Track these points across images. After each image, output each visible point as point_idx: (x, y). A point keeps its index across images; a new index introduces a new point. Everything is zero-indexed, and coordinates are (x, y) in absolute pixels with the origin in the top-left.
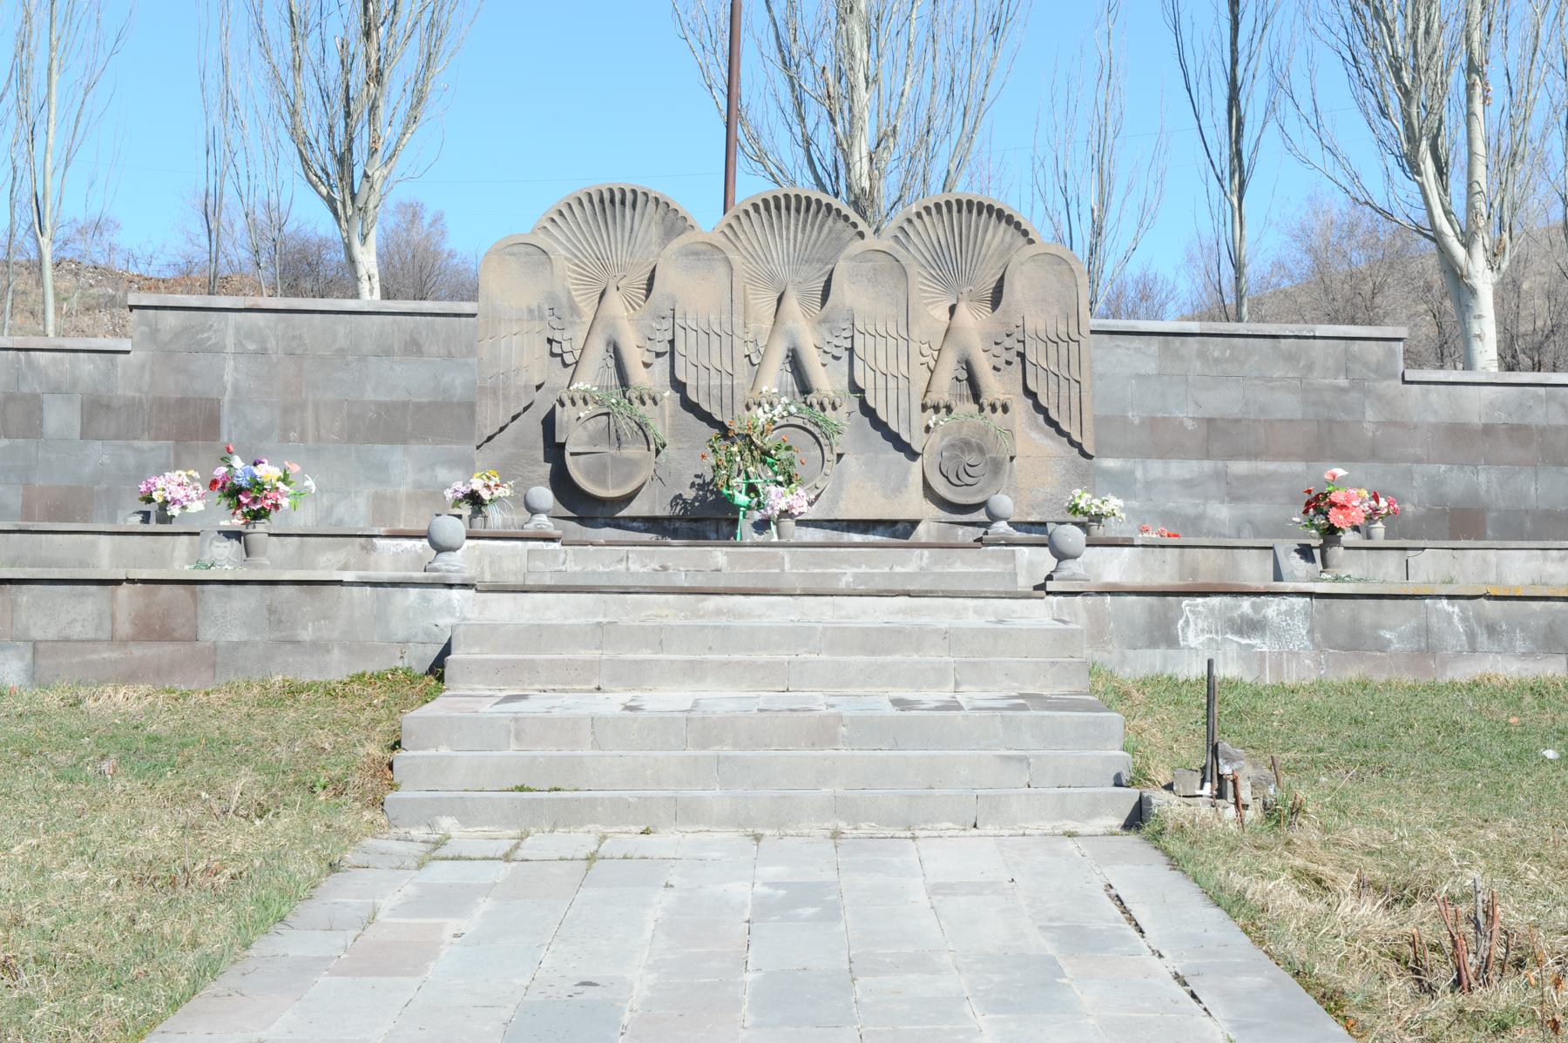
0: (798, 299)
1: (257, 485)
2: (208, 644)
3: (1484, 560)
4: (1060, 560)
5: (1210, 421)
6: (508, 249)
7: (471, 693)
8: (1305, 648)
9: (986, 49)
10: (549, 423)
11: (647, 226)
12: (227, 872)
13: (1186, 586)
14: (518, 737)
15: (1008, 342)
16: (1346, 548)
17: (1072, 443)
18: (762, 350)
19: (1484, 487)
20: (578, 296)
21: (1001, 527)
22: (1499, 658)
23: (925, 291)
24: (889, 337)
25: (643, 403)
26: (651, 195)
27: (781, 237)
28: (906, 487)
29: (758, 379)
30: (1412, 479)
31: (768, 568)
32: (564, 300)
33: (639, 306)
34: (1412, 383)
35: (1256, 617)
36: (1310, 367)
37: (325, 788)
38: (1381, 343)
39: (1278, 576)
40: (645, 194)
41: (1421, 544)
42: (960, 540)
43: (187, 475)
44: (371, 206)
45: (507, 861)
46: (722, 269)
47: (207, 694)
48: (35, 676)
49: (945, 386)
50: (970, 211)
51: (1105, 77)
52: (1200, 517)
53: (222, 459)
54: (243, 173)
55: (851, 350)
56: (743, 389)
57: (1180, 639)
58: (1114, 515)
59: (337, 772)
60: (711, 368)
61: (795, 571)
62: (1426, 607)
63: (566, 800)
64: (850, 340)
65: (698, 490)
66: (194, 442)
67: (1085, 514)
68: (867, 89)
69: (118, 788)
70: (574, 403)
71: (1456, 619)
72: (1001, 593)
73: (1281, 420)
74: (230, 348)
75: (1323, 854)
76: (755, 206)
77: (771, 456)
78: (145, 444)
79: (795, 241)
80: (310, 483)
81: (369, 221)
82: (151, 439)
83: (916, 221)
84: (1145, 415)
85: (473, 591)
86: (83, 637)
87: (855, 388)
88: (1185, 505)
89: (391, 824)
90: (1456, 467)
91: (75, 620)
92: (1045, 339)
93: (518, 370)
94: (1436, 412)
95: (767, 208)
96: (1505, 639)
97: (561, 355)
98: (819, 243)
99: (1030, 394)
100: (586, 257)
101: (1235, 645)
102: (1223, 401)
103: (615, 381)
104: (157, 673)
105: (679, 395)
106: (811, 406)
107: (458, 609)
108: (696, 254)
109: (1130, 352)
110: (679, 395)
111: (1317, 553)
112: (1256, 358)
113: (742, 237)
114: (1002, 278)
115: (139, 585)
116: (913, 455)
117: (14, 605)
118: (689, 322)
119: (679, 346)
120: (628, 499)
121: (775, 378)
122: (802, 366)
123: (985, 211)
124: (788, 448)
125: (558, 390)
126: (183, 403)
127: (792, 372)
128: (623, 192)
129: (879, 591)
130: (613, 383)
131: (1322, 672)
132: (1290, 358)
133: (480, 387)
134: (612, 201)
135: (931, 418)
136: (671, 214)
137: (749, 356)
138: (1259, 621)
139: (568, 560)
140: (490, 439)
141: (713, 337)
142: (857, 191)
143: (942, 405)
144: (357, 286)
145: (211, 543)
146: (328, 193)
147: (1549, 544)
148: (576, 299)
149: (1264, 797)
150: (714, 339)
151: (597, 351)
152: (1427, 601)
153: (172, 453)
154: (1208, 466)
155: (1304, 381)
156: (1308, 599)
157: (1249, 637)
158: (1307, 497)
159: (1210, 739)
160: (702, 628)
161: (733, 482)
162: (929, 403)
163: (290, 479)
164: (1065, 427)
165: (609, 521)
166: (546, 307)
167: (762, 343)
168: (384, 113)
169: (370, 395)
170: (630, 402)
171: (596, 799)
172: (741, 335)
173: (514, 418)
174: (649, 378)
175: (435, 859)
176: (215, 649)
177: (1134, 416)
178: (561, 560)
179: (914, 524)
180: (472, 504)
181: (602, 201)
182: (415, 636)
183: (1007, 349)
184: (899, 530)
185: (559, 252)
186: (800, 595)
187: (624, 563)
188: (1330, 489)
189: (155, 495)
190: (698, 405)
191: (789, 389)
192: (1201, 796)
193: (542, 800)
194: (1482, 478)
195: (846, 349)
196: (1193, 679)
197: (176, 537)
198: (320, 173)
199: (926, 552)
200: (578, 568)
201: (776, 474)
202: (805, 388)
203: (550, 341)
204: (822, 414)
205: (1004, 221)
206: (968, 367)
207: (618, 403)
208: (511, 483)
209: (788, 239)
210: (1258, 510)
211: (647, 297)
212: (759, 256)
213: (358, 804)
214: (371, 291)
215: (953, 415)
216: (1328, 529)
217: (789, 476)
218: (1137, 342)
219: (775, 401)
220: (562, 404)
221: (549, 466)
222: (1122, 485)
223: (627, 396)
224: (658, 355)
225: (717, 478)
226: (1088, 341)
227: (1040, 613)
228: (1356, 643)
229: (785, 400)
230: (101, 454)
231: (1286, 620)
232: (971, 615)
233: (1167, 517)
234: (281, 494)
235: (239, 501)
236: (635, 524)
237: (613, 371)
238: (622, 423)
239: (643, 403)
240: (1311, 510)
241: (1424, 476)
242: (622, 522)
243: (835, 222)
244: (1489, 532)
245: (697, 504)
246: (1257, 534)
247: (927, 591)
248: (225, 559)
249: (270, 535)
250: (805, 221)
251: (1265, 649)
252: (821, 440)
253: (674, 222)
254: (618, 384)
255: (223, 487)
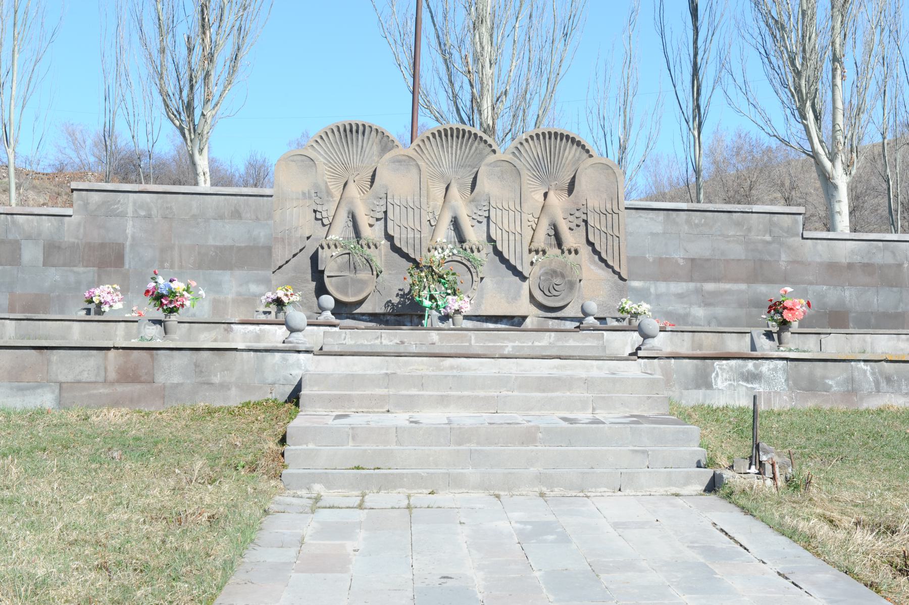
0: (458, 188)
1: (172, 293)
2: (160, 385)
3: (864, 340)
4: (644, 339)
5: (693, 260)
6: (291, 158)
7: (315, 413)
8: (784, 390)
9: (559, 45)
10: (314, 259)
11: (371, 145)
12: (206, 515)
13: (717, 353)
14: (354, 438)
15: (578, 214)
16: (792, 333)
17: (614, 272)
18: (437, 217)
19: (848, 299)
20: (331, 185)
21: (590, 320)
22: (893, 396)
23: (530, 184)
24: (510, 211)
25: (369, 247)
26: (374, 127)
27: (448, 152)
28: (520, 297)
29: (435, 234)
30: (807, 294)
31: (462, 343)
32: (323, 187)
33: (367, 191)
34: (807, 239)
35: (756, 372)
36: (749, 230)
37: (243, 467)
38: (790, 216)
39: (753, 348)
40: (370, 127)
41: (829, 331)
42: (550, 327)
43: (113, 288)
44: (205, 132)
45: (361, 509)
46: (414, 171)
47: (161, 413)
48: (60, 402)
49: (541, 239)
50: (556, 138)
51: (628, 62)
52: (687, 315)
53: (152, 278)
54: (131, 113)
55: (488, 218)
56: (426, 240)
57: (713, 384)
58: (645, 313)
59: (250, 458)
60: (408, 227)
61: (478, 344)
62: (852, 366)
63: (386, 474)
64: (487, 212)
65: (401, 298)
66: (108, 269)
67: (628, 313)
68: (490, 67)
69: (128, 466)
70: (329, 247)
71: (868, 374)
72: (612, 357)
73: (733, 260)
74: (130, 214)
75: (830, 506)
76: (433, 134)
77: (444, 279)
78: (81, 269)
79: (456, 155)
80: (202, 292)
81: (204, 140)
82: (83, 266)
83: (525, 144)
84: (656, 256)
85: (312, 354)
86: (89, 380)
87: (490, 240)
88: (678, 308)
89: (287, 488)
90: (832, 287)
91: (84, 370)
92: (599, 212)
93: (296, 228)
94: (821, 256)
95: (440, 136)
96: (896, 385)
97: (321, 220)
98: (470, 156)
99: (590, 243)
101: (744, 388)
102: (700, 249)
103: (352, 235)
104: (131, 401)
105: (389, 243)
106: (465, 250)
107: (303, 365)
108: (399, 161)
109: (648, 220)
110: (389, 243)
111: (775, 336)
112: (719, 224)
113: (425, 152)
114: (574, 177)
115: (121, 350)
116: (524, 278)
117: (49, 362)
118: (395, 201)
119: (390, 215)
120: (360, 303)
121: (444, 233)
122: (460, 227)
123: (565, 138)
124: (454, 274)
125: (320, 240)
126: (103, 245)
127: (454, 230)
128: (357, 125)
129: (542, 356)
130: (352, 236)
131: (793, 403)
132: (738, 224)
133: (275, 238)
134: (351, 131)
135: (535, 258)
136: (385, 139)
137: (429, 221)
138: (758, 374)
139: (347, 337)
140: (280, 267)
141: (409, 209)
142: (485, 126)
143: (540, 250)
144: (197, 178)
145: (145, 327)
146: (180, 124)
147: (900, 331)
148: (331, 187)
149: (786, 474)
150: (410, 211)
151: (343, 217)
152: (852, 363)
153: (96, 275)
154: (692, 285)
155: (747, 237)
156: (785, 362)
157: (752, 383)
158: (770, 304)
159: (755, 441)
160: (446, 376)
161: (422, 293)
162: (533, 249)
163: (191, 290)
164: (610, 263)
165: (348, 315)
166: (313, 191)
167: (437, 213)
168: (213, 79)
169: (211, 242)
170: (362, 246)
171: (403, 474)
172: (425, 209)
173: (294, 256)
174: (372, 233)
175: (319, 508)
176: (164, 387)
177: (650, 257)
178: (343, 338)
179: (524, 318)
180: (277, 305)
181: (345, 130)
182: (278, 381)
183: (577, 218)
184: (515, 321)
185: (320, 160)
186: (498, 358)
187: (379, 339)
188: (783, 299)
189: (94, 299)
190: (400, 249)
191: (453, 240)
192: (749, 473)
193: (372, 474)
194: (847, 293)
195: (485, 217)
196: (721, 407)
197: (117, 323)
198: (175, 113)
199: (553, 334)
200: (353, 342)
201: (447, 289)
202: (462, 240)
203: (315, 211)
204: (472, 254)
205: (575, 144)
206: (555, 227)
207: (355, 247)
208: (300, 293)
209: (452, 154)
210: (720, 311)
211: (371, 186)
212: (435, 163)
213: (265, 477)
214: (205, 181)
215: (547, 255)
216: (782, 322)
217: (454, 290)
218: (651, 213)
219: (445, 247)
220: (323, 248)
221: (314, 283)
222: (641, 295)
223: (360, 243)
224: (378, 220)
225: (413, 291)
226: (624, 213)
227: (634, 368)
228: (813, 387)
229: (450, 246)
230: (54, 275)
231: (773, 374)
232: (596, 370)
233: (668, 315)
234: (185, 298)
235: (161, 302)
236: (364, 317)
237: (351, 229)
238: (357, 258)
239: (369, 247)
240: (772, 311)
241: (814, 293)
242: (356, 316)
243: (479, 144)
244: (851, 325)
245: (400, 306)
246: (720, 324)
247: (570, 356)
248: (153, 335)
249: (179, 322)
250: (462, 143)
251: (761, 390)
252: (472, 269)
253: (386, 143)
254: (354, 236)
255: (152, 294)
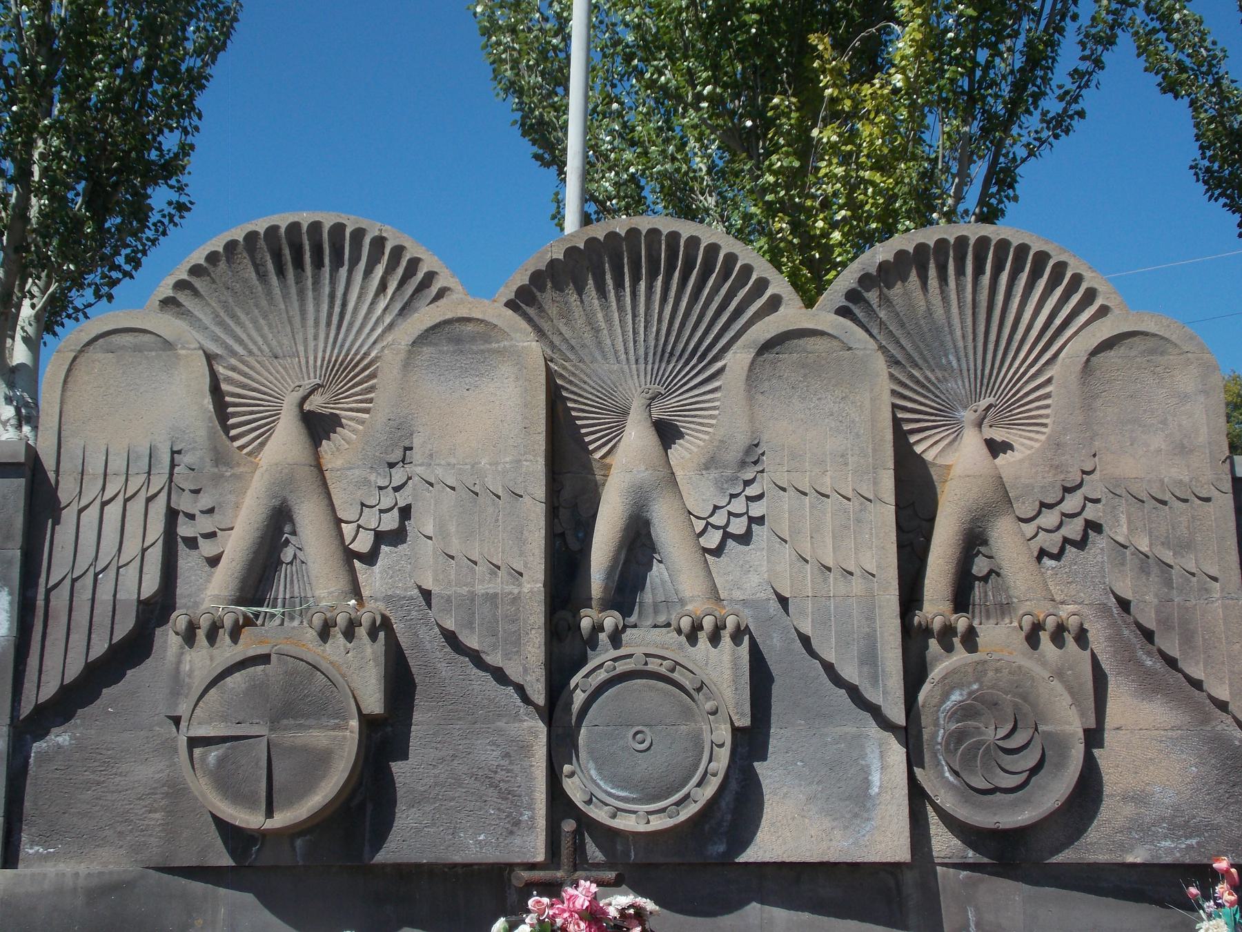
100: (251, 353)
137: (562, 535)
141: (485, 499)
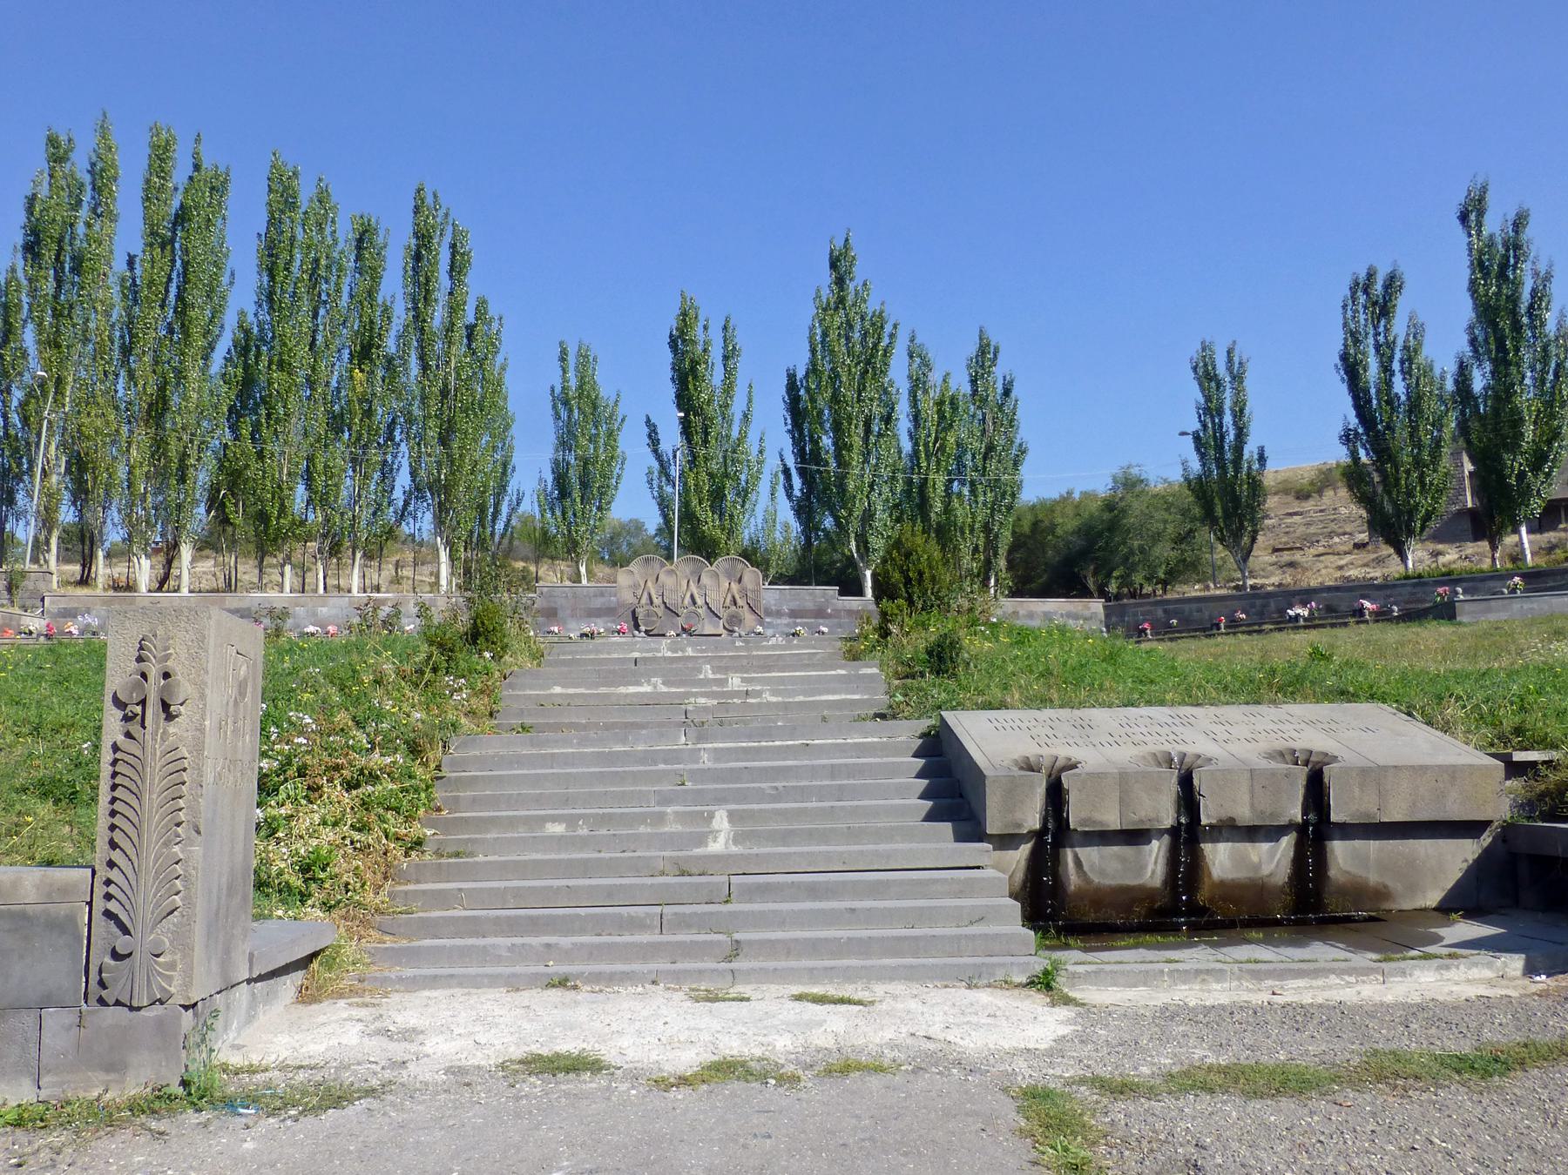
102: (794, 605)
116: (720, 618)
121: (688, 599)
132: (811, 594)
151: (645, 596)
154: (791, 620)
206: (734, 597)
